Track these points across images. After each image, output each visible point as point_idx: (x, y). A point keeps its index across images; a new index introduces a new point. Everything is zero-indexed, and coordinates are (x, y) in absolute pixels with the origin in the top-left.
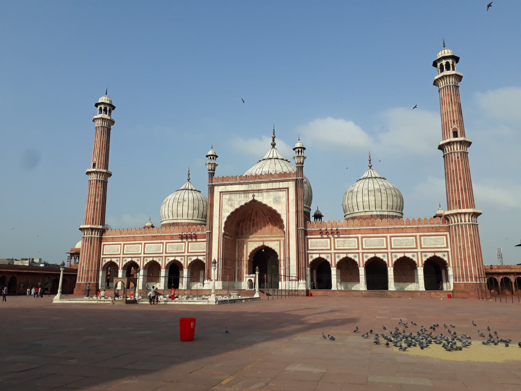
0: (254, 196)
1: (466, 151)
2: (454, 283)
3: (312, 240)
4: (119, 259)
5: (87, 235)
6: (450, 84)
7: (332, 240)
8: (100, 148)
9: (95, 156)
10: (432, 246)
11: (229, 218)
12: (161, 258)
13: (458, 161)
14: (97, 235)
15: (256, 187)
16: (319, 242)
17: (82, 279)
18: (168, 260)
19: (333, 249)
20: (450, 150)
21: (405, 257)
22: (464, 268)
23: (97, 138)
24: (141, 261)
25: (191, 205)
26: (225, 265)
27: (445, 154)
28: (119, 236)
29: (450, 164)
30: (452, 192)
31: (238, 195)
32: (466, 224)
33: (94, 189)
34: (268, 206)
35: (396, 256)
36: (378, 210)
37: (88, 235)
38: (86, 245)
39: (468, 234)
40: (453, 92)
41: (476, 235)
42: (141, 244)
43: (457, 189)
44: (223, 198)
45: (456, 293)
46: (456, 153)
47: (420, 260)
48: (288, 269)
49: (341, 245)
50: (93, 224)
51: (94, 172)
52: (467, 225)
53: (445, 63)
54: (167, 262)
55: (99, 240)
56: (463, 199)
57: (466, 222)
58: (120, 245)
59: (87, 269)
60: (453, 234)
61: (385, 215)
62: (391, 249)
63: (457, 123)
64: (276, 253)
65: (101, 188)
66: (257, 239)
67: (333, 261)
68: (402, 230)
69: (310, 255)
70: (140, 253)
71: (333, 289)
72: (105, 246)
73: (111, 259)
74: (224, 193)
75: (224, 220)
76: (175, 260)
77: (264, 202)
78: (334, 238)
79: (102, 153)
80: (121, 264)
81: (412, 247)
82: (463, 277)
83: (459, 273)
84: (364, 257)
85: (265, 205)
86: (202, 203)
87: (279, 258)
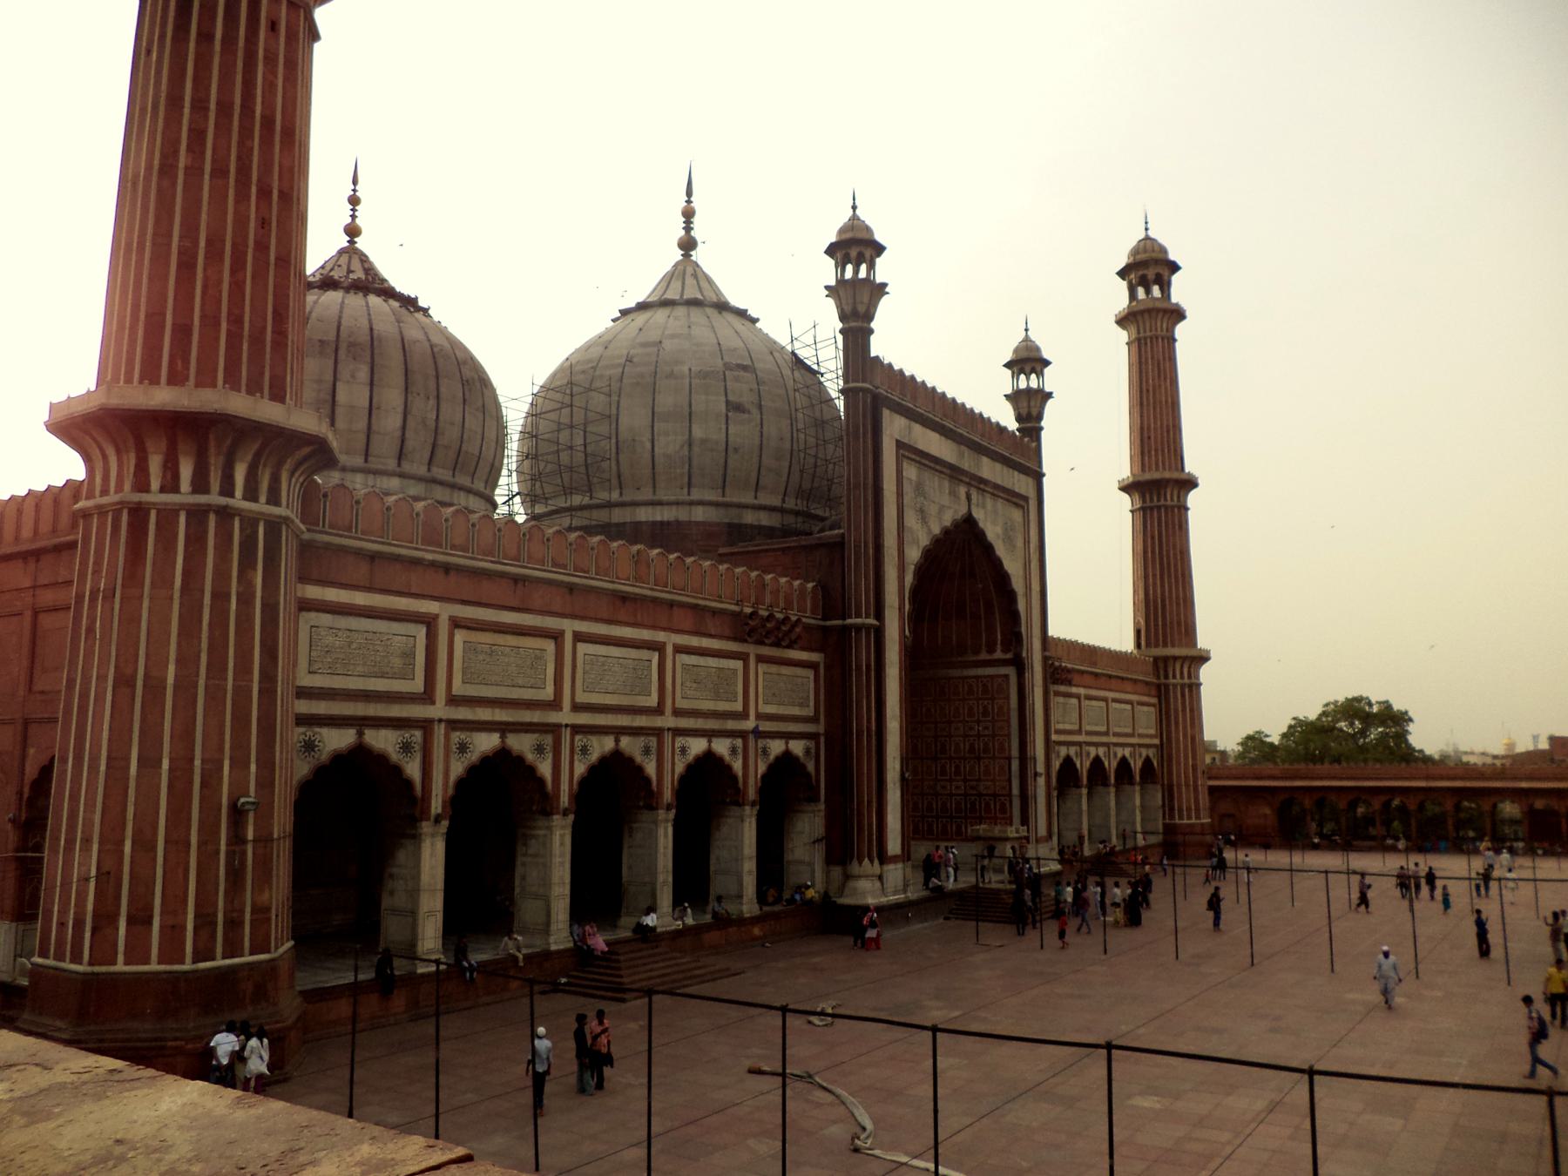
2: (1164, 824)
5: (251, 494)
17: (233, 924)
20: (1175, 499)
27: (1162, 502)
28: (429, 557)
29: (1174, 533)
30: (1178, 604)
37: (263, 499)
38: (246, 600)
42: (557, 636)
60: (1176, 705)
73: (360, 734)
75: (909, 578)
83: (1188, 801)
85: (988, 549)
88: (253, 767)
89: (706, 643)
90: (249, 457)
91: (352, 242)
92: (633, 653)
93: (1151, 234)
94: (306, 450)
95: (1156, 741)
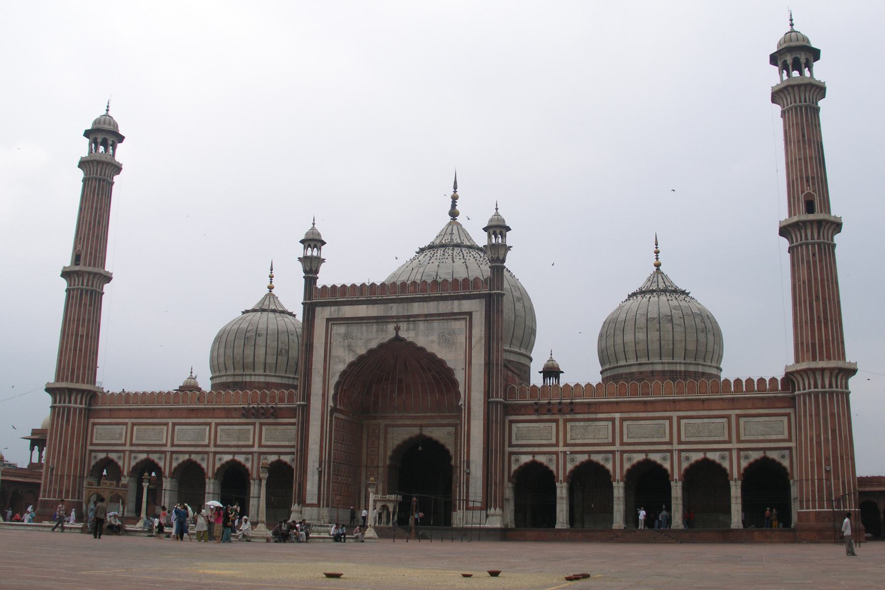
0: (397, 329)
1: (830, 242)
3: (520, 425)
4: (122, 454)
5: (60, 402)
6: (800, 104)
7: (560, 424)
8: (90, 223)
9: (80, 239)
10: (761, 438)
11: (344, 374)
12: (206, 456)
13: (815, 262)
14: (81, 403)
15: (404, 310)
16: (534, 430)
18: (220, 459)
19: (561, 444)
20: (799, 240)
21: (705, 461)
22: (816, 481)
23: (86, 202)
24: (165, 460)
25: (272, 344)
26: (337, 475)
29: (798, 266)
30: (801, 326)
31: (364, 328)
32: (824, 393)
33: (75, 308)
34: (428, 351)
35: (687, 458)
36: (666, 361)
37: (62, 402)
39: (829, 412)
40: (807, 121)
41: (844, 415)
42: (167, 424)
43: (810, 320)
44: (334, 332)
45: (801, 533)
46: (810, 246)
47: (735, 467)
48: (465, 486)
49: (579, 437)
50: (72, 381)
51: (77, 273)
52: (827, 395)
53: (792, 61)
54: (218, 465)
55: (85, 414)
56: (820, 340)
57: (825, 388)
58: (125, 427)
59: (59, 474)
60: (800, 412)
61: (680, 372)
62: (678, 444)
63: (813, 184)
64: (447, 452)
65: (90, 305)
66: (408, 422)
67: (562, 469)
68: (703, 403)
69: (513, 458)
70: (165, 443)
71: (558, 526)
72: (96, 427)
73: (107, 454)
74: (336, 322)
76: (233, 461)
77: (421, 342)
78: (566, 421)
79: (94, 232)
80: (126, 465)
81: (722, 439)
82: (814, 500)
83: (807, 492)
84: (625, 460)
85: (422, 350)
86: (296, 341)
87: (453, 463)
88: (56, 460)
89: (231, 420)
90: (58, 394)
91: (270, 291)
92: (198, 427)
93: (795, 28)
94: (66, 391)
95: (792, 444)
